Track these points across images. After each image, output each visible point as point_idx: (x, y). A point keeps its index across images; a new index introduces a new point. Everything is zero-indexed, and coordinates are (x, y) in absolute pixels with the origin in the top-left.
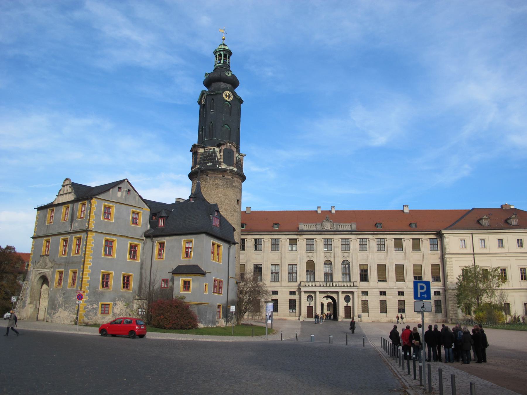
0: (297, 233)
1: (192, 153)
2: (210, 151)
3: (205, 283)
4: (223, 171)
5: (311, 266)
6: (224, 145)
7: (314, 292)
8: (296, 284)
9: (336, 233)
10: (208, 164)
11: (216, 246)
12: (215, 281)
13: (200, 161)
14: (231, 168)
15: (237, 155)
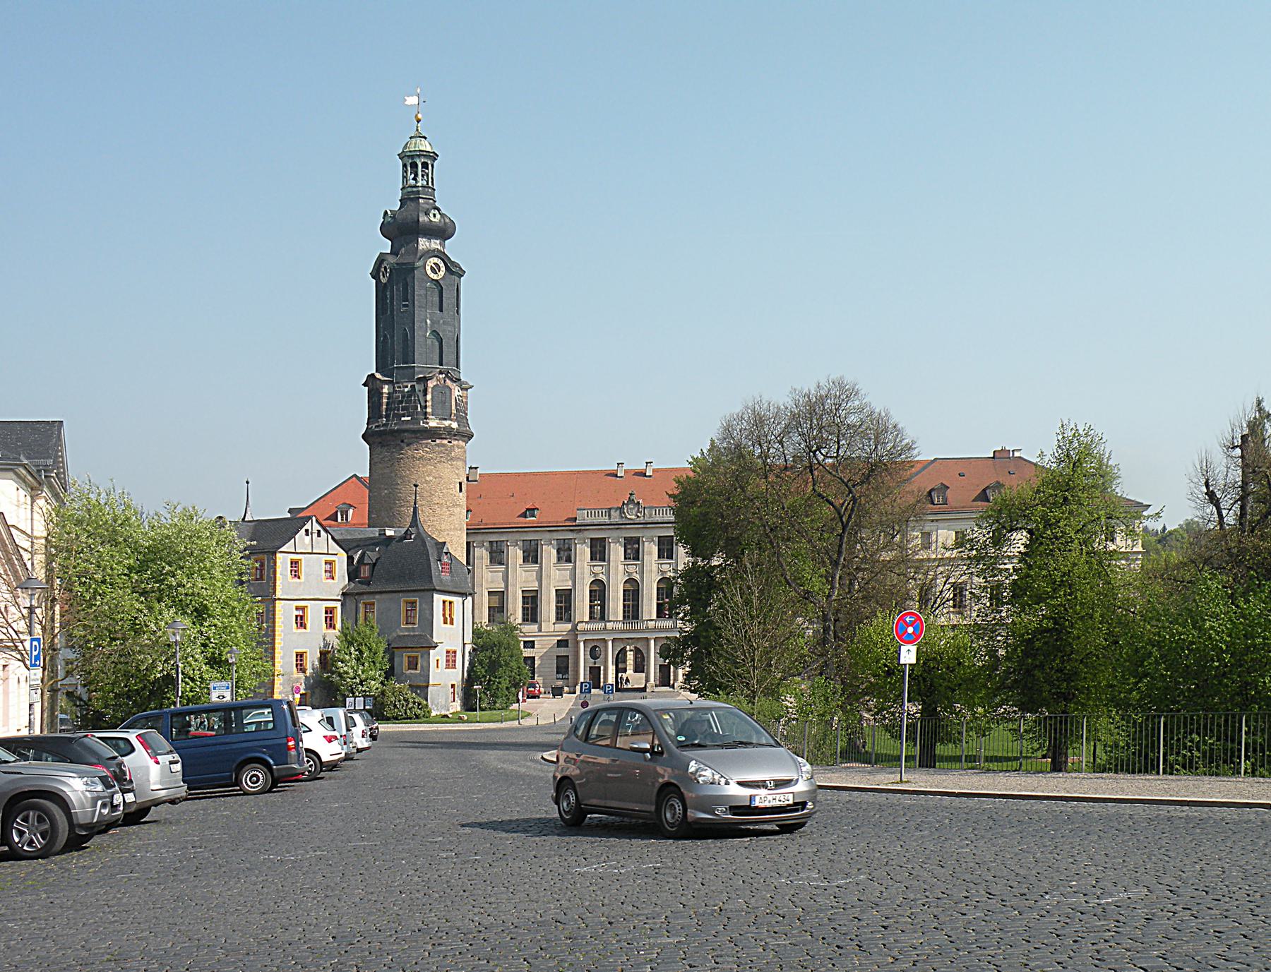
0: (572, 528)
1: (367, 388)
2: (406, 390)
3: (437, 658)
4: (434, 434)
5: (599, 592)
6: (431, 378)
7: (605, 641)
8: (569, 626)
9: (648, 526)
10: (403, 419)
11: (447, 604)
12: (448, 652)
13: (387, 409)
14: (447, 423)
15: (456, 392)
